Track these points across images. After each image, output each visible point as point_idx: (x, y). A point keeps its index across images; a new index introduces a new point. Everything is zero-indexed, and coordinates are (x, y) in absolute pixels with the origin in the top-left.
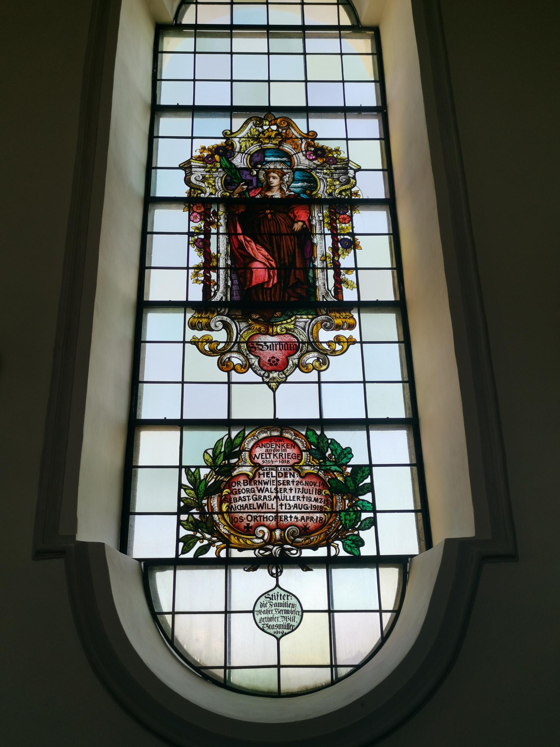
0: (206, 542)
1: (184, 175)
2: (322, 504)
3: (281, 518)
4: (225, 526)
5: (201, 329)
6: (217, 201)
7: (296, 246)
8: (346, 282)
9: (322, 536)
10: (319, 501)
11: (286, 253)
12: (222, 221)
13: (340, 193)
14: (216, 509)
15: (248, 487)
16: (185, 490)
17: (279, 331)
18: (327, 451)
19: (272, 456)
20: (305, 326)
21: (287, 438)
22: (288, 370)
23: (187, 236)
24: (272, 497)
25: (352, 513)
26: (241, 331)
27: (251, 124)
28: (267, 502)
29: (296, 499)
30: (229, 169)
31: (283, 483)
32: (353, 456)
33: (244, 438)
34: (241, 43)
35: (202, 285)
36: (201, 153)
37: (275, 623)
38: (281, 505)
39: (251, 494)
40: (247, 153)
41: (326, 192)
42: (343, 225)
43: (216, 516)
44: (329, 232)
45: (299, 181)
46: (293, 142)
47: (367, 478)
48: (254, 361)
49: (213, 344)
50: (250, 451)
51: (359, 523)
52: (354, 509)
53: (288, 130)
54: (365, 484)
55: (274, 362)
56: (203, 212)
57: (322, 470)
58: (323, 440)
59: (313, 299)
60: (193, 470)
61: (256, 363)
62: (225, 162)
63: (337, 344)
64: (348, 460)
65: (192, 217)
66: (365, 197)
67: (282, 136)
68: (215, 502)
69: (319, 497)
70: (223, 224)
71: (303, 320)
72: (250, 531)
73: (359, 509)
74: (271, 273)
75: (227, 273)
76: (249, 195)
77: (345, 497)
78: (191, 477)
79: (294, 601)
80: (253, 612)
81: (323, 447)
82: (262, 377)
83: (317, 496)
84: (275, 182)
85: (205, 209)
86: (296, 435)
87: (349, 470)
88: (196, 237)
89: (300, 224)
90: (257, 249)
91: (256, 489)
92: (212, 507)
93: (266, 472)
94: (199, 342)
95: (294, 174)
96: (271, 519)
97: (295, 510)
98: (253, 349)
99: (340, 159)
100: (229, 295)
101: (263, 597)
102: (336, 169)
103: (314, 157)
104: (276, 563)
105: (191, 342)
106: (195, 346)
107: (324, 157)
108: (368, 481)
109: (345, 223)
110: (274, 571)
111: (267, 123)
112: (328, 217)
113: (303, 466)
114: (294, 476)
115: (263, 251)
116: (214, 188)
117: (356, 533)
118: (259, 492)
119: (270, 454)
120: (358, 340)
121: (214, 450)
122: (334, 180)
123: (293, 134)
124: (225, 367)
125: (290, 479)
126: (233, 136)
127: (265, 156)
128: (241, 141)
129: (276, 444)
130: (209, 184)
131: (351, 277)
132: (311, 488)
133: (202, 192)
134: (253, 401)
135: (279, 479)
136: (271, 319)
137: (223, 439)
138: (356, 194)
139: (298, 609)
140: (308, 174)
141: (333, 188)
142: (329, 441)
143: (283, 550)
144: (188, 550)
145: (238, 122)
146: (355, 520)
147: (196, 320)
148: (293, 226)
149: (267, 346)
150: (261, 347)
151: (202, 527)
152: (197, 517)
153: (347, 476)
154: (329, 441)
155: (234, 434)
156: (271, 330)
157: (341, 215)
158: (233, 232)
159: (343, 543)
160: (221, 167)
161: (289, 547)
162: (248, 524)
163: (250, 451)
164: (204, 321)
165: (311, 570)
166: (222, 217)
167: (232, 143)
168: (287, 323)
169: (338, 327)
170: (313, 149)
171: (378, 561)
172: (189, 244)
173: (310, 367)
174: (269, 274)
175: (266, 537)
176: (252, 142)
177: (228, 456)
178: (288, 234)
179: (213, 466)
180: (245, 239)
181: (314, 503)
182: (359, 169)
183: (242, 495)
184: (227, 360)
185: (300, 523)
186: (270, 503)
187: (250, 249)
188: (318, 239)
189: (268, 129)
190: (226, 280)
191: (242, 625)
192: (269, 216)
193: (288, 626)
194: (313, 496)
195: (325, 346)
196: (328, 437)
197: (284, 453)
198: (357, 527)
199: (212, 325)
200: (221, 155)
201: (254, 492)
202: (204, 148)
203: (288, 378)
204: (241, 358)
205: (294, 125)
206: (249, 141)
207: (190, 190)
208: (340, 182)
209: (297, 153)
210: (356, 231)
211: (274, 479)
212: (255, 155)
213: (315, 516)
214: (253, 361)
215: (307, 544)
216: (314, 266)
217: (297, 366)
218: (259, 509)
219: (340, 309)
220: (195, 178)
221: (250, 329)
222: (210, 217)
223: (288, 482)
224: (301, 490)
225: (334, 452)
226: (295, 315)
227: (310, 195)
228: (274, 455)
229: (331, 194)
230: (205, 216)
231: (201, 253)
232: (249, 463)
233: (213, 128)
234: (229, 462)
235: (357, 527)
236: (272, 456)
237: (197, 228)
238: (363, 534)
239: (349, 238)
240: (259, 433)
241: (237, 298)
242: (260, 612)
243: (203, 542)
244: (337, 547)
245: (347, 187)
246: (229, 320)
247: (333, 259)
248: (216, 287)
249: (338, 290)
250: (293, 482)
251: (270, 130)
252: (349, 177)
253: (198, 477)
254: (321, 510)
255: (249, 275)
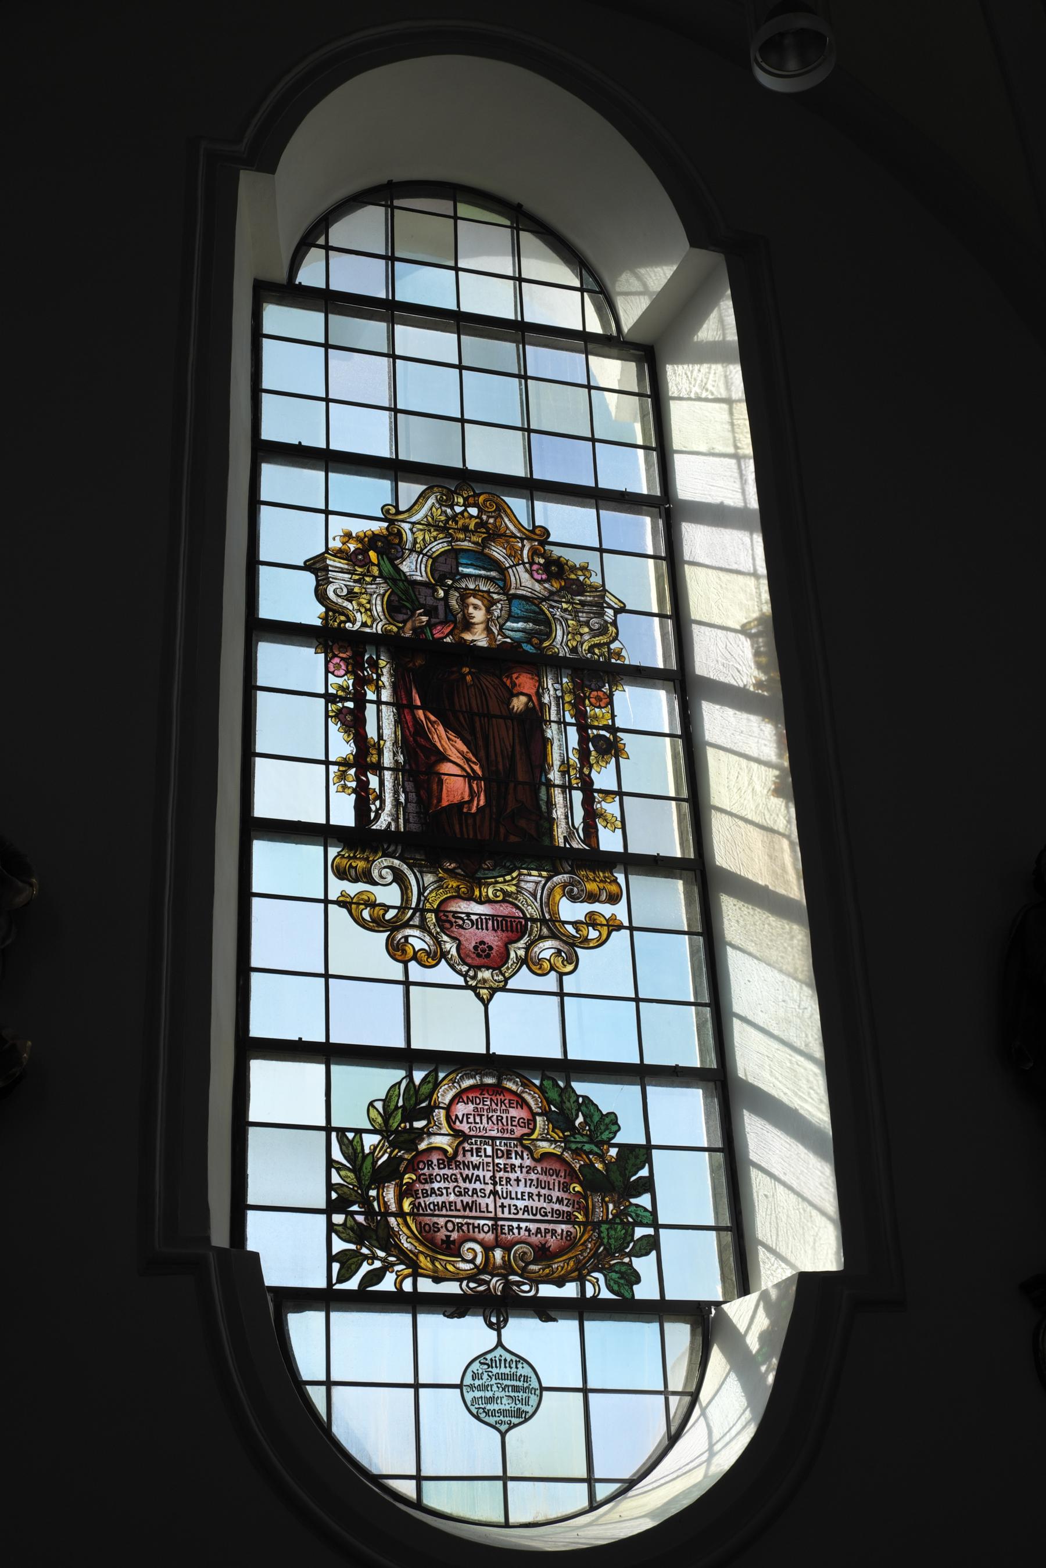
0: (378, 1264)
1: (315, 583)
2: (569, 1209)
3: (502, 1229)
4: (408, 1237)
5: (355, 880)
6: (375, 640)
7: (517, 741)
8: (601, 815)
9: (572, 1263)
10: (565, 1202)
11: (498, 751)
12: (385, 679)
13: (591, 649)
14: (393, 1208)
15: (446, 1171)
16: (338, 1170)
17: (490, 895)
18: (577, 1116)
19: (485, 1119)
20: (536, 890)
21: (510, 1091)
22: (508, 969)
23: (322, 701)
24: (487, 1192)
25: (620, 1227)
26: (425, 889)
27: (431, 501)
28: (480, 1200)
29: (526, 1197)
30: (394, 581)
31: (505, 1168)
32: (619, 1129)
33: (437, 1085)
34: (411, 339)
35: (353, 796)
36: (344, 544)
37: (496, 1407)
38: (503, 1206)
39: (452, 1185)
40: (425, 555)
41: (567, 645)
42: (597, 710)
43: (392, 1220)
44: (573, 721)
45: (517, 619)
46: (508, 542)
47: (643, 1167)
48: (450, 946)
49: (377, 908)
50: (448, 1109)
51: (631, 1245)
52: (622, 1220)
53: (499, 520)
54: (640, 1178)
55: (484, 951)
56: (350, 658)
57: (570, 1149)
58: (570, 1097)
59: (547, 842)
60: (350, 1135)
61: (454, 951)
62: (387, 567)
63: (590, 928)
64: (611, 1135)
65: (331, 666)
66: (635, 662)
67: (488, 529)
68: (390, 1194)
69: (565, 1196)
70: (387, 684)
71: (532, 880)
72: (452, 1248)
73: (631, 1220)
74: (475, 786)
75: (396, 779)
76: (433, 635)
77: (607, 1199)
78: (347, 1148)
79: (526, 1371)
80: (459, 1386)
81: (570, 1110)
82: (465, 976)
83: (561, 1194)
84: (478, 615)
85: (354, 653)
86: (524, 1085)
87: (613, 1152)
88: (340, 705)
89: (523, 699)
90: (449, 739)
91: (459, 1176)
92: (385, 1203)
93: (475, 1147)
94: (351, 903)
95: (510, 604)
96: (486, 1229)
97: (526, 1216)
98: (448, 925)
99: (590, 586)
100: (401, 821)
101: (477, 1363)
102: (583, 603)
103: (544, 577)
104: (497, 1306)
105: (337, 902)
106: (344, 911)
107: (562, 579)
108: (644, 1172)
109: (600, 707)
110: (494, 1320)
111: (461, 500)
112: (570, 692)
113: (537, 1140)
114: (522, 1158)
115: (460, 744)
116: (370, 616)
117: (626, 1260)
118: (465, 1182)
119: (481, 1116)
120: (626, 923)
121: (386, 1101)
122: (581, 624)
123: (507, 527)
124: (399, 953)
125: (517, 1162)
126: (400, 517)
127: (458, 564)
128: (415, 530)
129: (491, 1100)
130: (360, 605)
131: (611, 808)
132: (551, 1179)
133: (349, 620)
134: (449, 1021)
135: (497, 1161)
136: (476, 872)
137: (400, 1083)
138: (618, 654)
139: (535, 1384)
140: (534, 607)
141: (578, 638)
142: (581, 1100)
143: (508, 1284)
144: (347, 1276)
145: (410, 491)
146: (624, 1238)
147: (345, 861)
148: (509, 702)
149: (471, 921)
150: (461, 922)
151: (371, 1237)
152: (360, 1219)
153: (610, 1162)
154: (581, 1100)
155: (418, 1076)
156: (477, 893)
157: (593, 690)
158: (405, 702)
159: (605, 1276)
160: (381, 576)
161: (517, 1278)
162: (448, 1237)
163: (448, 1109)
164: (361, 864)
165: (555, 1320)
166: (385, 671)
167: (399, 530)
168: (505, 881)
169: (592, 898)
170: (542, 561)
171: (662, 1310)
172: (327, 716)
173: (546, 965)
174: (471, 787)
175: (478, 1261)
176: (435, 534)
177: (410, 1114)
178: (501, 717)
179: (383, 1131)
180: (426, 717)
181: (557, 1206)
182: (623, 610)
183: (436, 1185)
184: (403, 940)
185: (535, 1240)
186: (483, 1202)
187: (435, 736)
188: (555, 732)
189: (462, 513)
190: (396, 793)
191: (444, 1410)
192: (469, 678)
193: (519, 1413)
194: (556, 1194)
195: (570, 928)
196: (578, 1093)
197: (504, 1116)
198: (627, 1250)
199: (375, 874)
200: (379, 553)
201: (456, 1180)
202: (348, 536)
203: (509, 982)
204: (428, 939)
205: (509, 511)
206: (429, 531)
207: (327, 613)
208: (591, 630)
209: (515, 566)
210: (619, 724)
211: (490, 1160)
212: (442, 559)
213: (560, 1228)
214: (448, 946)
215: (547, 1275)
216: (549, 780)
217: (524, 961)
218: (465, 1210)
219: (593, 866)
220: (335, 591)
221: (441, 887)
222: (363, 669)
223: (513, 1167)
224: (535, 1182)
225: (588, 1120)
226: (519, 869)
227: (538, 647)
228: (489, 1119)
229: (574, 650)
230: (355, 666)
231: (349, 735)
232: (445, 1129)
233: (365, 497)
234: (411, 1125)
235: (627, 1250)
236: (485, 1119)
237: (341, 688)
238: (638, 1263)
239: (608, 735)
240: (462, 1078)
241: (414, 827)
242: (471, 1387)
243: (373, 1263)
244: (596, 1283)
245: (603, 639)
246: (405, 868)
247: (581, 771)
248: (378, 803)
249: (591, 831)
250: (521, 1167)
251: (466, 514)
252: (606, 622)
253: (359, 1149)
254: (569, 1219)
255: (435, 786)
